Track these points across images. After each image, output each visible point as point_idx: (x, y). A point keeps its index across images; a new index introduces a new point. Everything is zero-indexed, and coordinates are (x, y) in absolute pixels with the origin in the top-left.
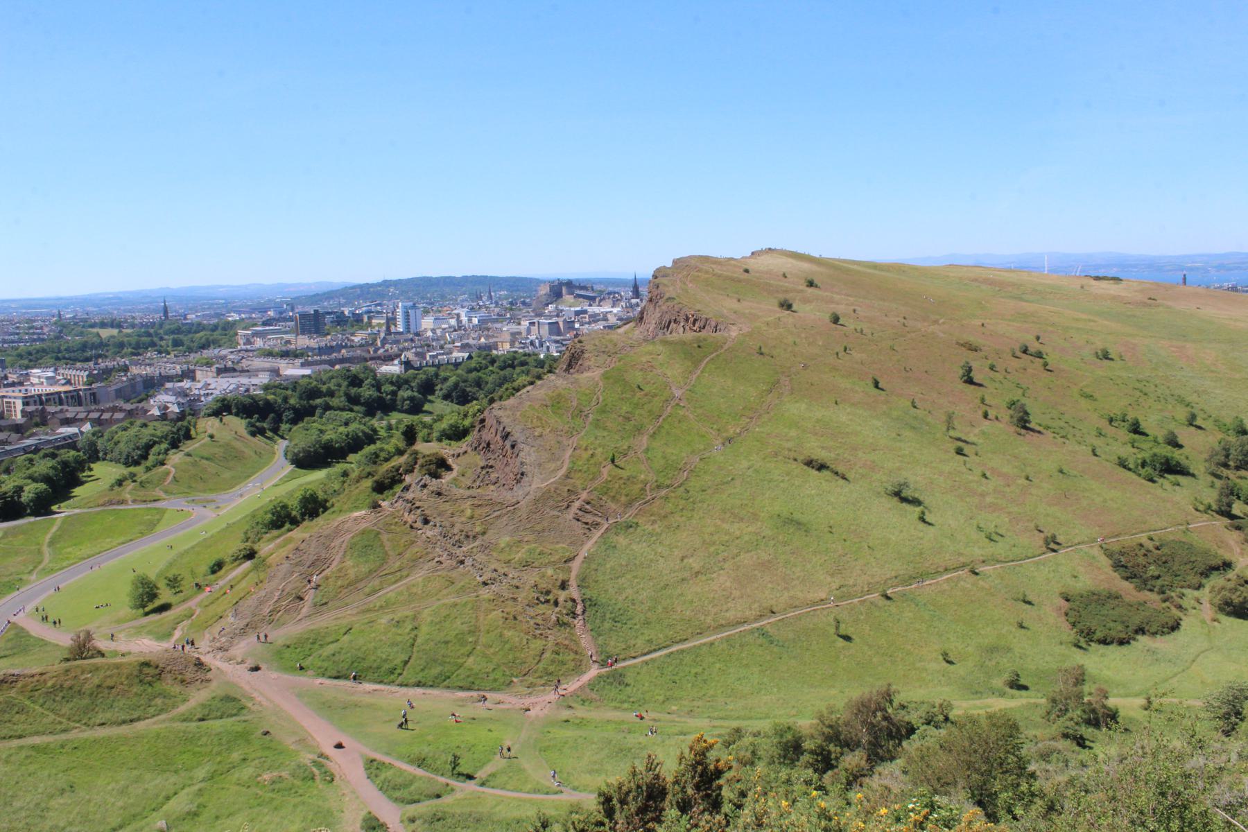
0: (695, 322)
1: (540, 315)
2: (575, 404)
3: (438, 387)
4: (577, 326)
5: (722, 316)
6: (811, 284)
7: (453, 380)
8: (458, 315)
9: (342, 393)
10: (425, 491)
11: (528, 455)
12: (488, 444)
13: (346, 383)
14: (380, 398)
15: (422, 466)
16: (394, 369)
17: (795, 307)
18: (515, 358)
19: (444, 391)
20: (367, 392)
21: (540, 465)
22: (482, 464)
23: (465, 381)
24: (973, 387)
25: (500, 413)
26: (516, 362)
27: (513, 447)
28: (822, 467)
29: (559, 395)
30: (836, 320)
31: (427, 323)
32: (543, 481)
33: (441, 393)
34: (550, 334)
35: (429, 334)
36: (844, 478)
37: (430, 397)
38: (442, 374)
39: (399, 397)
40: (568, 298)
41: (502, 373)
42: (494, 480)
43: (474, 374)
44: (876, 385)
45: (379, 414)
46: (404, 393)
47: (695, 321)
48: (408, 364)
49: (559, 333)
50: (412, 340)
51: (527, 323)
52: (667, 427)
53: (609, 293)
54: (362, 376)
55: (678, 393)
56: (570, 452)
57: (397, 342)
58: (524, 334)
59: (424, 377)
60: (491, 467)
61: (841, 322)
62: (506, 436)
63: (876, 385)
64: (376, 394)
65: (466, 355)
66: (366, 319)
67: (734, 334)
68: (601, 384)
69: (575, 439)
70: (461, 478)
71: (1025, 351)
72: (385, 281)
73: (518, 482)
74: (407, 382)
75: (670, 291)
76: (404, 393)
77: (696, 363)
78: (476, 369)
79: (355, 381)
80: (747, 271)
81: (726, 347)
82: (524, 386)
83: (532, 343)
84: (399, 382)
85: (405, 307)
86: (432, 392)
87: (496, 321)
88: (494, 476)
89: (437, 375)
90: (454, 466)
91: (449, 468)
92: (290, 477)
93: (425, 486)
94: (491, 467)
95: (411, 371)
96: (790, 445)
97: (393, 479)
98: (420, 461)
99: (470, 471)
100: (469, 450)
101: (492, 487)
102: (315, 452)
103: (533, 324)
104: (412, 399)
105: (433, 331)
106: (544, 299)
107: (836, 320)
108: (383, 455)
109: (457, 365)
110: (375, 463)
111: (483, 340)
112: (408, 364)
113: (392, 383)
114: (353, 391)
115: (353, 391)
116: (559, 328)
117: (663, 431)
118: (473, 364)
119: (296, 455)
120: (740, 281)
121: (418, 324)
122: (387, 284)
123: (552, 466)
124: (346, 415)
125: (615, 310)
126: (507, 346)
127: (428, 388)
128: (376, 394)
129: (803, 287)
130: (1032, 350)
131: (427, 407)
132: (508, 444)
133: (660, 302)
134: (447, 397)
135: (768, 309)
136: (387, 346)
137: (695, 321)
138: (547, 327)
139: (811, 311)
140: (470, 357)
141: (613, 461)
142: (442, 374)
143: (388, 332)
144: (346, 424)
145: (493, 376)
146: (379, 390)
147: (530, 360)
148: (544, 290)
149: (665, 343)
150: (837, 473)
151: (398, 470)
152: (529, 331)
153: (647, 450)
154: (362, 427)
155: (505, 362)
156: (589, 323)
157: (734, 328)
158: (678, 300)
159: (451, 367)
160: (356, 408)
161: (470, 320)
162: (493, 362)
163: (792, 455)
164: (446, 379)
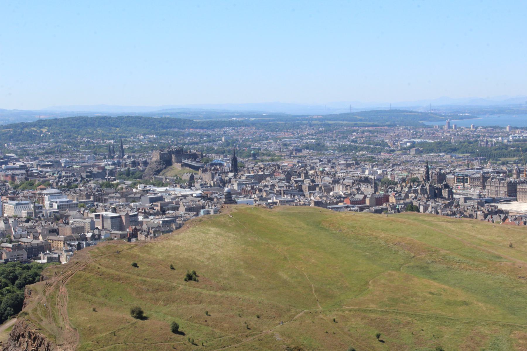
34: (112, 227)
49: (121, 228)
72: (40, 121)
103: (97, 216)
106: (154, 166)
116: (121, 221)
122: (41, 124)
138: (109, 221)
139: (160, 318)
148: (155, 157)
161: (51, 205)
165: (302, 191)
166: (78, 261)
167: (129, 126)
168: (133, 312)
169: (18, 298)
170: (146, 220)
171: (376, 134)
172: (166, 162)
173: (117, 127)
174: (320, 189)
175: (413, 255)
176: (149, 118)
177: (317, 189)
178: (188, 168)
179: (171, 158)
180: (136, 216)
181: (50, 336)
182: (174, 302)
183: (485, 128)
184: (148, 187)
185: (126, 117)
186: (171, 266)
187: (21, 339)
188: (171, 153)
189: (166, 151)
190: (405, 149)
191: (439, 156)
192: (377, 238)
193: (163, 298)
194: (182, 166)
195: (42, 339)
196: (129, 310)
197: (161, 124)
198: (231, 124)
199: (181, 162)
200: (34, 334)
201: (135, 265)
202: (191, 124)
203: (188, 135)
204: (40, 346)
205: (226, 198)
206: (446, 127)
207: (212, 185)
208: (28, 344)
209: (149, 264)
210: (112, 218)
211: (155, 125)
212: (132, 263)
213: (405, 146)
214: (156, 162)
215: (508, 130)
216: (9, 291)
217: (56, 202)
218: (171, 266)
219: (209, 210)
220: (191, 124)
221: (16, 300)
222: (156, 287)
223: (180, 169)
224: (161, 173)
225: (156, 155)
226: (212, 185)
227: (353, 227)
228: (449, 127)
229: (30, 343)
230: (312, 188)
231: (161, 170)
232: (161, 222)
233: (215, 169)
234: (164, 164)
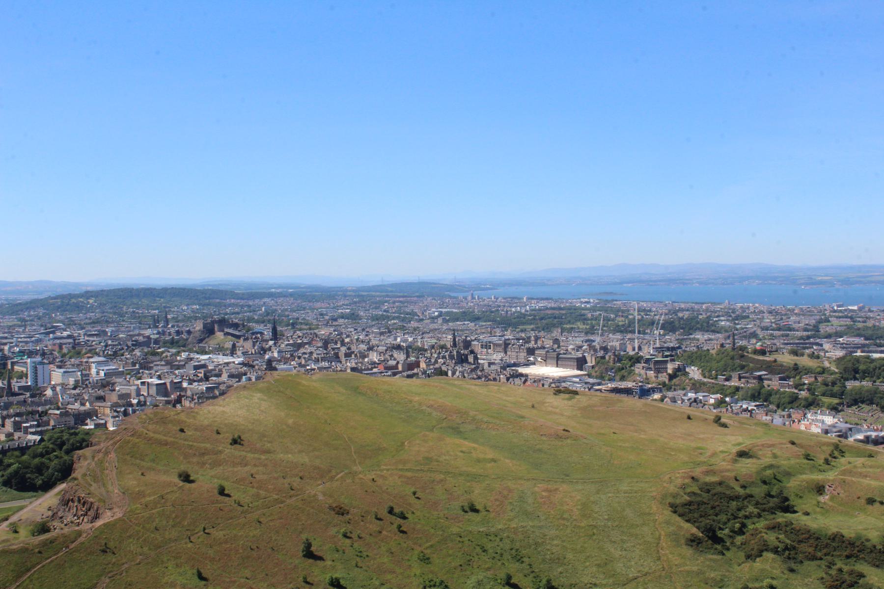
7: (15, 466)
19: (5, 478)
24: (311, 561)
34: (157, 394)
40: (219, 335)
43: (37, 460)
49: (166, 394)
65: (38, 438)
66: (9, 367)
71: (391, 511)
72: (87, 292)
78: (42, 455)
106: (197, 334)
109: (23, 450)
116: (166, 388)
130: (397, 510)
138: (155, 388)
139: (206, 480)
140: (42, 440)
148: (199, 326)
159: (17, 453)
161: (98, 373)
164: (9, 465)
168: (180, 476)
172: (209, 331)
174: (356, 355)
175: (445, 416)
180: (180, 382)
181: (100, 500)
182: (220, 465)
184: (192, 355)
187: (71, 504)
188: (213, 322)
189: (209, 320)
192: (411, 401)
195: (92, 503)
198: (271, 295)
199: (223, 331)
201: (182, 430)
203: (230, 305)
209: (196, 430)
210: (157, 385)
216: (57, 457)
223: (222, 337)
227: (389, 392)
230: (348, 355)
231: (204, 339)
233: (256, 338)
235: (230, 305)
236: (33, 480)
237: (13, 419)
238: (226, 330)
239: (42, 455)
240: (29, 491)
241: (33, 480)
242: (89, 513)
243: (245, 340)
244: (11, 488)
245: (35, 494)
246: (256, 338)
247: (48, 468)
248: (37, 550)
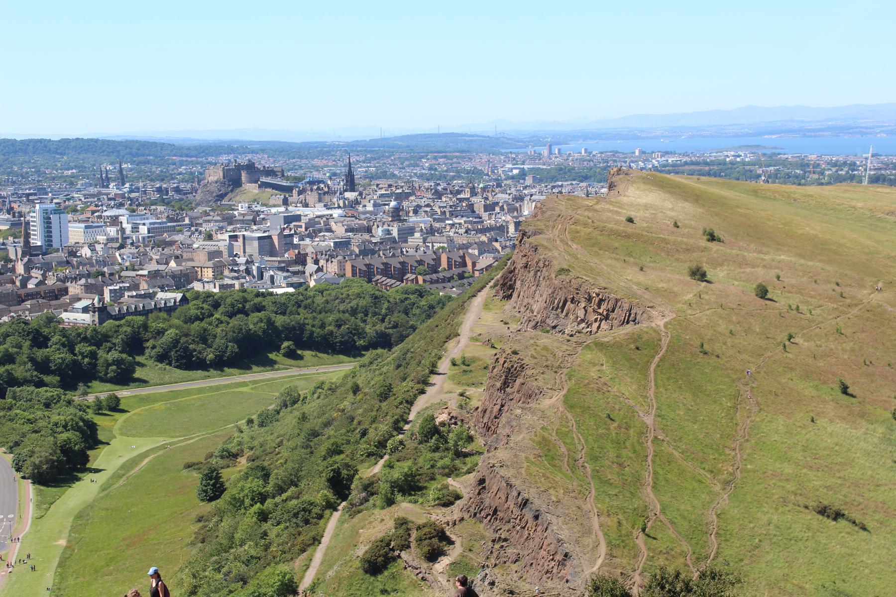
0: (605, 307)
1: (230, 220)
2: (563, 449)
3: (149, 344)
4: (296, 240)
5: (634, 296)
6: (712, 238)
7: (171, 333)
8: (115, 221)
9: (24, 358)
10: (495, 589)
11: (561, 529)
12: (495, 511)
13: (28, 343)
14: (75, 362)
15: (420, 540)
16: (77, 317)
17: (709, 277)
18: (245, 300)
19: (157, 349)
20: (56, 354)
21: (577, 542)
22: (490, 534)
23: (186, 335)
25: (503, 472)
26: (248, 306)
27: (536, 517)
28: (838, 516)
29: (544, 438)
30: (763, 293)
31: (75, 233)
32: (592, 562)
33: (153, 353)
34: (261, 252)
35: (86, 252)
36: (864, 528)
37: (139, 359)
38: (154, 325)
39: (101, 361)
40: (251, 189)
41: (235, 322)
42: (514, 558)
44: (845, 390)
45: (81, 387)
46: (107, 356)
47: (601, 301)
48: (103, 312)
49: (272, 252)
50: (68, 262)
51: (226, 236)
52: (661, 472)
53: (312, 183)
54: (45, 331)
55: (649, 420)
56: (595, 522)
57: (47, 268)
58: (225, 254)
59: (129, 329)
60: (505, 540)
61: (769, 296)
62: (525, 503)
63: (845, 390)
64: (69, 357)
65: (179, 296)
67: (660, 323)
68: (570, 416)
69: (591, 500)
70: (471, 555)
73: (562, 564)
74: (106, 338)
75: (559, 257)
76: (107, 356)
77: (645, 370)
78: (197, 318)
79: (39, 340)
80: (630, 220)
81: (664, 343)
82: (415, 396)
83: (248, 272)
84: (98, 339)
85: (45, 211)
86: (141, 352)
87: (173, 230)
88: (511, 551)
89: (145, 327)
90: (453, 538)
91: (451, 542)
92: (44, 505)
93: (492, 584)
94: (505, 540)
95: (109, 323)
96: (791, 486)
97: (386, 555)
98: (414, 534)
99: (477, 545)
100: (466, 516)
101: (514, 567)
102: (57, 461)
104: (118, 362)
105: (92, 246)
106: (214, 188)
107: (763, 293)
108: (316, 510)
109: (170, 310)
110: (307, 522)
111: (173, 264)
112: (103, 312)
113: (85, 339)
114: (40, 354)
115: (40, 354)
117: (661, 478)
118: (192, 309)
119: (37, 467)
120: (628, 237)
121: (63, 235)
123: (588, 541)
124: (45, 393)
125: (336, 213)
126: (208, 274)
127: (135, 345)
128: (69, 357)
129: (703, 242)
131: (139, 373)
132: (528, 515)
133: (545, 273)
134: (162, 358)
135: (672, 276)
136: (37, 274)
137: (601, 301)
138: (256, 244)
140: (184, 300)
141: (644, 530)
142: (154, 325)
143: (29, 251)
144: (47, 406)
145: (222, 327)
146: (72, 351)
147: (267, 302)
148: (214, 175)
149: (600, 346)
150: (854, 522)
151: (388, 544)
152: (231, 248)
153: (663, 510)
154: (72, 410)
155: (232, 305)
156: (310, 236)
157: (654, 313)
158: (572, 274)
159: (163, 315)
160: (47, 379)
161: (135, 229)
162: (216, 305)
163: (802, 500)
164: (160, 333)
165: (473, 212)
166: (557, 213)
167: (79, 153)
169: (241, 329)
170: (301, 242)
171: (455, 160)
172: (233, 180)
173: (62, 154)
174: (502, 209)
176: (109, 141)
177: (497, 209)
178: (269, 190)
179: (241, 175)
180: (291, 236)
183: (602, 153)
185: (73, 140)
186: (676, 223)
188: (239, 168)
190: (513, 178)
191: (572, 184)
193: (705, 259)
194: (260, 187)
195: (617, 301)
196: (687, 271)
197: (128, 150)
199: (256, 182)
200: (598, 295)
202: (172, 151)
204: (613, 311)
205: (392, 217)
206: (545, 152)
207: (342, 205)
208: (586, 311)
210: (260, 238)
211: (119, 151)
212: (624, 219)
213: (510, 174)
214: (216, 182)
215: (637, 153)
217: (144, 224)
218: (676, 223)
219: (390, 228)
220: (172, 151)
221: (239, 333)
222: (684, 246)
223: (256, 191)
224: (226, 198)
225: (215, 172)
226: (342, 205)
228: (550, 153)
229: (590, 310)
231: (226, 194)
232: (332, 244)
233: (318, 189)
234: (229, 185)
235: (181, 164)
236: (200, 353)
237: (83, 281)
238: (264, 179)
239: (197, 318)
240: (197, 369)
241: (200, 353)
242: (612, 315)
243: (300, 193)
244: (170, 364)
245: (207, 373)
246: (318, 189)
247: (215, 336)
248: (632, 346)
